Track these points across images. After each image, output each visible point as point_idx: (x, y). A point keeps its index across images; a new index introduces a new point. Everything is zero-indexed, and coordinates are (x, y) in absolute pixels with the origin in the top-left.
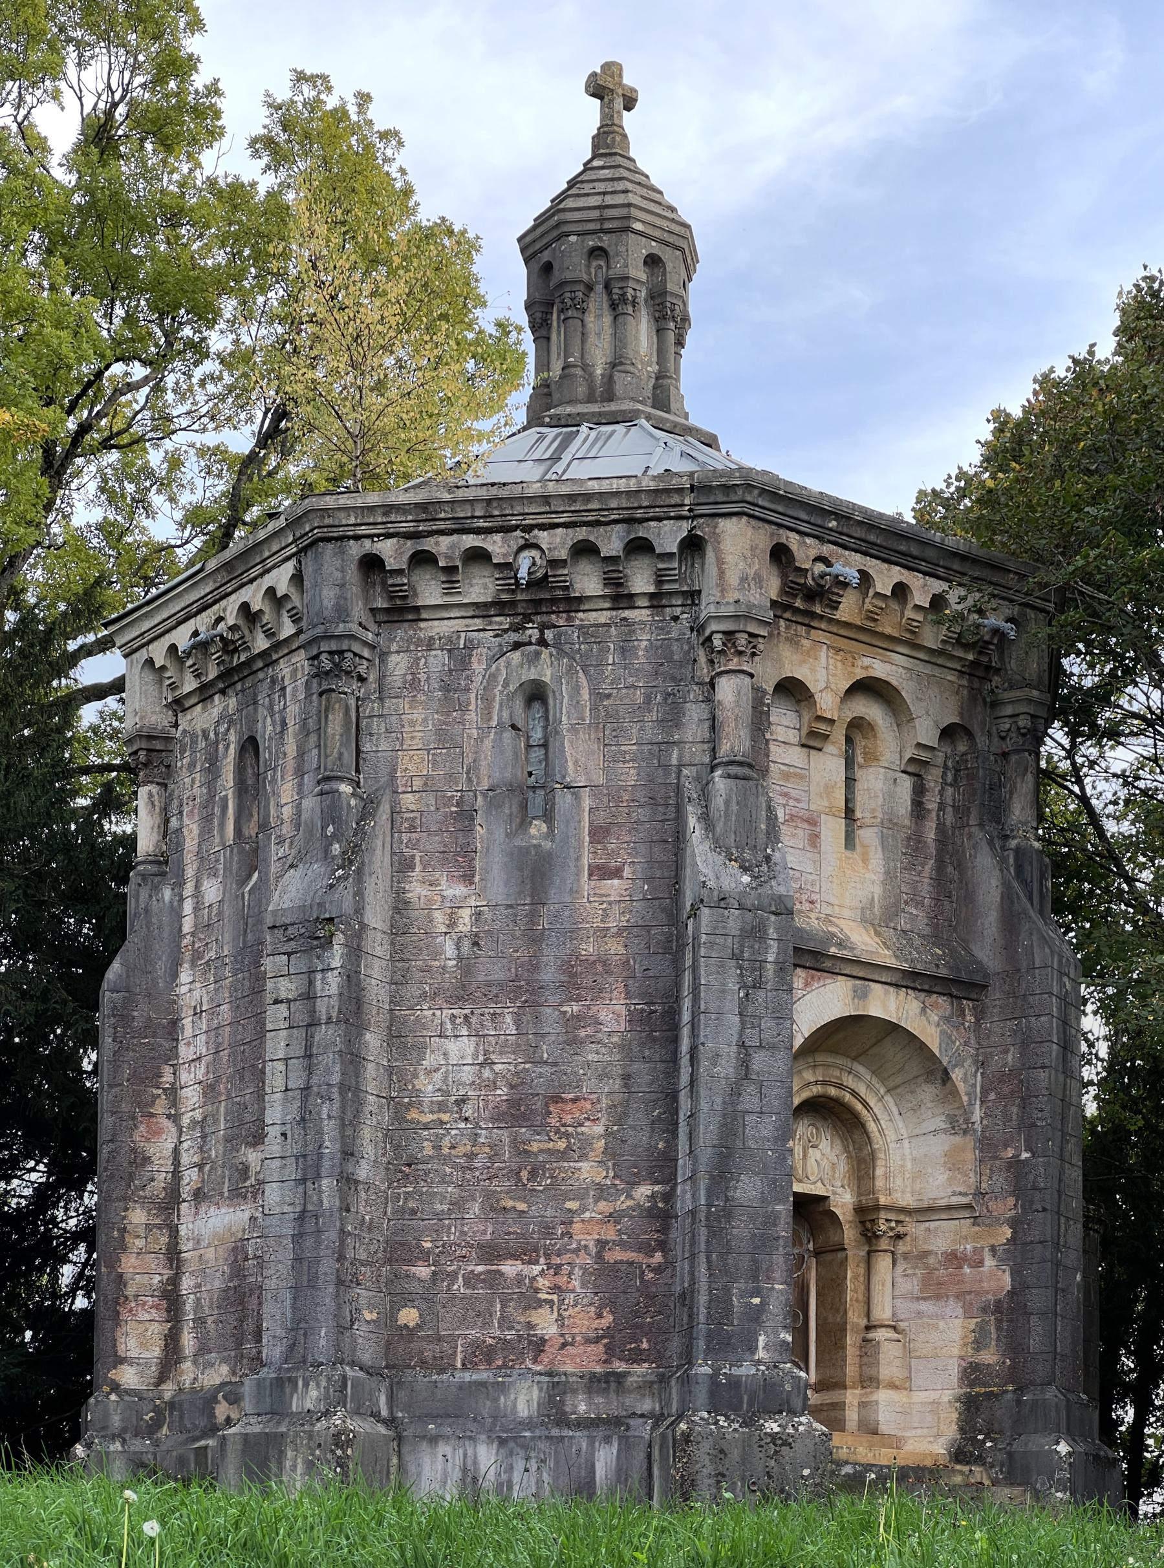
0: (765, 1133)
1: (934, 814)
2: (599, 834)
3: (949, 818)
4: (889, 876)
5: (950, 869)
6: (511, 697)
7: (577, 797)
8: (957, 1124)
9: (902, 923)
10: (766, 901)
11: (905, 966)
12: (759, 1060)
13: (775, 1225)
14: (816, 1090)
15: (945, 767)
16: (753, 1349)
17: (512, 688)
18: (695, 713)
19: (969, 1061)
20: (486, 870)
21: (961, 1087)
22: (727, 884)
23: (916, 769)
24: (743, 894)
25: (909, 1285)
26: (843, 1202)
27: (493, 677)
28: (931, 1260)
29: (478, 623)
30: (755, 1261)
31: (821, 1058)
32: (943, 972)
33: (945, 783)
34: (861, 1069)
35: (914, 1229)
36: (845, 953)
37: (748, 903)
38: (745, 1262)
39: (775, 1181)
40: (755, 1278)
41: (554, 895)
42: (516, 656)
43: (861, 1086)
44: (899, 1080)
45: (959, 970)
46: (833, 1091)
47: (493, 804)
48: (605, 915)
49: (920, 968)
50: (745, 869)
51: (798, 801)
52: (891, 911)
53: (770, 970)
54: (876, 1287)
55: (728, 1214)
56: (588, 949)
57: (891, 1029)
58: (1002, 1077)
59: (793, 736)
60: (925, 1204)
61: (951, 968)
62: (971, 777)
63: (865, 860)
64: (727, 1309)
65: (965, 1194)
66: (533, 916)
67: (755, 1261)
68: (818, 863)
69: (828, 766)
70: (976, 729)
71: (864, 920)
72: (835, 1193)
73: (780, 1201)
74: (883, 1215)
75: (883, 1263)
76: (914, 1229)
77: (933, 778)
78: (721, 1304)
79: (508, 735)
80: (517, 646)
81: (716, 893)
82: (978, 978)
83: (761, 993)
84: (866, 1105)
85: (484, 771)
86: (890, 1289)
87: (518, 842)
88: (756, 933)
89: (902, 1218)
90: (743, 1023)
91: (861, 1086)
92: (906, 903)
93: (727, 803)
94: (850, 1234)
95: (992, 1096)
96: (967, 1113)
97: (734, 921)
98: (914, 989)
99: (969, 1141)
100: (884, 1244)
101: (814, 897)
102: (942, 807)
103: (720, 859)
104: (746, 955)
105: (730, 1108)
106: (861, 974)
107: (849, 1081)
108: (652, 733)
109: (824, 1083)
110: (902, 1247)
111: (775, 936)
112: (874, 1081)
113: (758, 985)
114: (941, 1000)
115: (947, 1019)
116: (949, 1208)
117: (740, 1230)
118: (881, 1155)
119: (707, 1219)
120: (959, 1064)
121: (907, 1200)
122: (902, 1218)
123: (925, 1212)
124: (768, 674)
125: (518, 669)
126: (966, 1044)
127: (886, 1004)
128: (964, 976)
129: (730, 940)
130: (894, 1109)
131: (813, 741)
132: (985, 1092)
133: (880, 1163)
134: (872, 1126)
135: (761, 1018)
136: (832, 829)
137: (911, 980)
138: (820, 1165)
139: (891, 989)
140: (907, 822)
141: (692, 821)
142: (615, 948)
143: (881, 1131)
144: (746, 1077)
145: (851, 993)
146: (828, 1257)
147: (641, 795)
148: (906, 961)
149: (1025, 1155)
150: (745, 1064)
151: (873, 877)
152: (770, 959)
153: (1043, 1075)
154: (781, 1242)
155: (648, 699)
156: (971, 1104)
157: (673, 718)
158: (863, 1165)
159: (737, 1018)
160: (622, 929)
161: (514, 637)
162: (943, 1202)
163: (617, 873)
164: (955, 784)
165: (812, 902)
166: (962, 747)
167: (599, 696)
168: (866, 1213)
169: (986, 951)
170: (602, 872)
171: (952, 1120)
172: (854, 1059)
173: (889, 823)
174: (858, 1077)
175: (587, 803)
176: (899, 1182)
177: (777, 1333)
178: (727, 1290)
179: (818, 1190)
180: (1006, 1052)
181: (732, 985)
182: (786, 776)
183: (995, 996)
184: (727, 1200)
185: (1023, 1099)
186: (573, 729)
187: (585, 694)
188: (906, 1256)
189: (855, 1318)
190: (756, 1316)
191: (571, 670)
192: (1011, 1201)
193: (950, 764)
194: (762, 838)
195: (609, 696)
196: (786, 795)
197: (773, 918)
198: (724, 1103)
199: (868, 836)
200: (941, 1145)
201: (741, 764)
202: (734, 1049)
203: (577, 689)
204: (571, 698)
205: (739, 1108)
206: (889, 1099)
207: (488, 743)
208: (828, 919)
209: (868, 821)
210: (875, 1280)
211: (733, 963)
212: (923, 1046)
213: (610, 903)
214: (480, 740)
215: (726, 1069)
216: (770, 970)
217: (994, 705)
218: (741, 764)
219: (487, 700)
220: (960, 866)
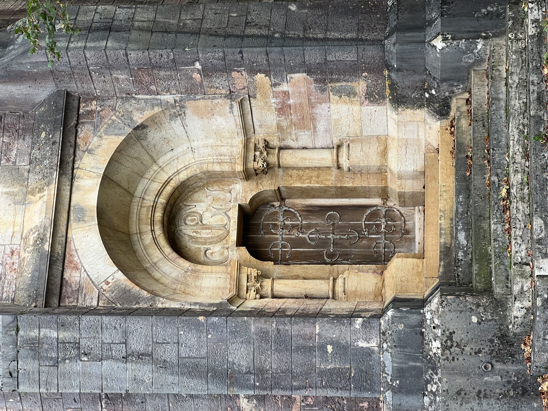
0: (194, 340)
8: (177, 111)
9: (24, 164)
10: (8, 339)
11: (55, 175)
12: (137, 344)
13: (267, 332)
14: (158, 231)
16: (369, 352)
19: (127, 105)
21: (148, 113)
25: (305, 138)
26: (243, 192)
28: (284, 124)
30: (298, 349)
31: (134, 228)
32: (58, 137)
34: (140, 188)
35: (260, 135)
36: (49, 235)
37: (12, 353)
38: (298, 358)
39: (232, 332)
40: (311, 349)
43: (151, 192)
44: (146, 157)
45: (56, 121)
46: (159, 215)
49: (56, 160)
53: (64, 335)
54: (307, 164)
55: (260, 372)
57: (107, 180)
58: (138, 82)
60: (241, 131)
61: (55, 129)
64: (339, 373)
65: (231, 107)
67: (298, 349)
71: (23, 202)
72: (236, 200)
73: (247, 328)
74: (251, 165)
75: (288, 158)
76: (260, 135)
78: (334, 378)
81: (5, 380)
82: (62, 103)
83: (83, 342)
84: (167, 183)
86: (308, 157)
88: (35, 346)
89: (252, 146)
90: (108, 358)
91: (151, 192)
92: (8, 160)
94: (267, 185)
95: (153, 88)
96: (167, 106)
97: (27, 365)
98: (74, 161)
99: (190, 105)
100: (273, 159)
101: (8, 251)
104: (54, 355)
105: (176, 369)
106: (65, 216)
107: (150, 199)
109: (152, 223)
110: (275, 142)
111: (36, 331)
112: (148, 176)
113: (77, 345)
114: (81, 135)
115: (96, 128)
116: (243, 115)
117: (273, 362)
118: (205, 168)
119: (265, 389)
120: (129, 115)
121: (239, 141)
122: (252, 146)
123: (246, 130)
126: (114, 109)
127: (87, 191)
128: (60, 117)
129: (43, 369)
130: (169, 155)
132: (150, 92)
133: (210, 168)
134: (183, 176)
135: (103, 343)
137: (66, 167)
138: (214, 216)
139: (76, 184)
143: (186, 168)
144: (150, 355)
145: (81, 224)
146: (284, 194)
148: (51, 174)
149: (198, 65)
150: (140, 356)
152: (55, 335)
153: (133, 55)
154: (281, 327)
156: (160, 104)
158: (212, 179)
159: (105, 363)
162: (239, 120)
165: (12, 253)
168: (248, 175)
169: (42, 92)
171: (174, 117)
172: (132, 195)
174: (145, 192)
176: (224, 150)
177: (355, 331)
178: (322, 373)
179: (234, 214)
180: (117, 79)
181: (78, 366)
183: (74, 87)
184: (249, 372)
185: (153, 68)
188: (281, 140)
189: (330, 180)
190: (342, 349)
192: (234, 74)
197: (21, 333)
198: (172, 374)
200: (193, 121)
202: (129, 365)
205: (175, 362)
206: (161, 161)
208: (25, 239)
210: (301, 164)
211: (61, 365)
212: (119, 151)
215: (145, 371)
216: (64, 335)
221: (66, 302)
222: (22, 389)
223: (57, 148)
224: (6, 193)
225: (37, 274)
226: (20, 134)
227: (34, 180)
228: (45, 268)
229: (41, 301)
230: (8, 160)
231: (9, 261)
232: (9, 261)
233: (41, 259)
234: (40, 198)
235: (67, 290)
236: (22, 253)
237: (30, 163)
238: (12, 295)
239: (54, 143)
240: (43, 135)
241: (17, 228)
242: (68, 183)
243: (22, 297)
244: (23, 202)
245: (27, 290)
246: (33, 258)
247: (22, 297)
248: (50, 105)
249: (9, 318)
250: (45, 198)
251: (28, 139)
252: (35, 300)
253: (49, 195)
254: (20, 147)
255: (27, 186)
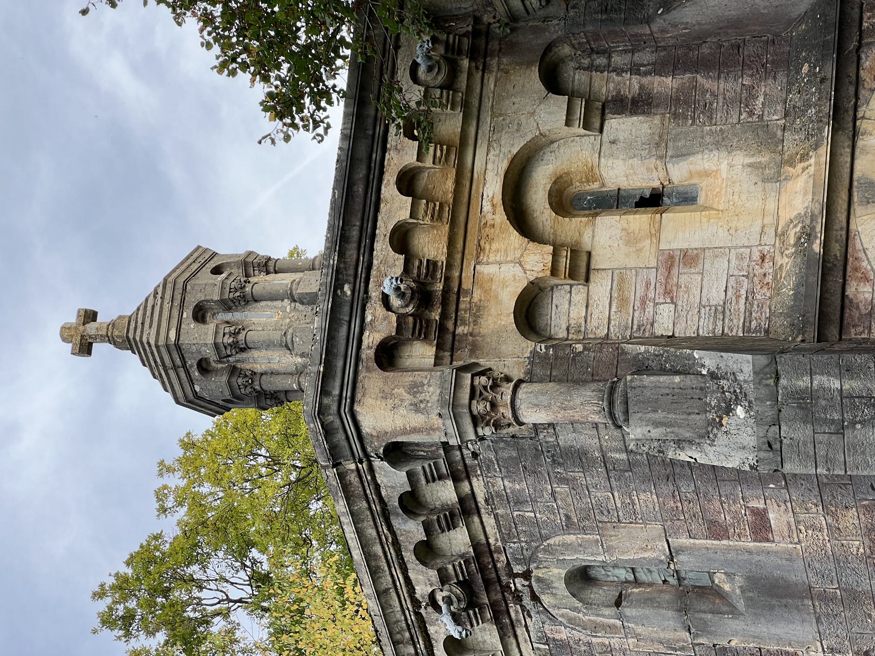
1: (646, 80)
2: (717, 531)
3: (646, 57)
4: (721, 143)
5: (705, 50)
6: (587, 604)
7: (681, 550)
9: (775, 118)
10: (763, 391)
11: (827, 131)
15: (591, 68)
17: (580, 605)
18: (566, 438)
20: (779, 640)
22: (749, 437)
23: (594, 113)
24: (759, 421)
27: (570, 620)
29: (521, 631)
32: (830, 70)
33: (608, 68)
36: (819, 228)
37: (770, 413)
41: (798, 575)
42: (546, 599)
47: (704, 629)
48: (813, 527)
49: (827, 108)
50: (729, 411)
51: (648, 284)
52: (765, 137)
56: (857, 545)
59: (579, 294)
61: (824, 58)
62: (597, 37)
63: (707, 174)
66: (826, 598)
68: (718, 251)
69: (607, 236)
70: (541, 41)
71: (778, 178)
77: (605, 85)
79: (628, 611)
80: (535, 598)
81: (762, 455)
85: (669, 635)
87: (741, 605)
88: (807, 404)
92: (751, 113)
93: (657, 424)
97: (795, 432)
98: (856, 108)
101: (756, 256)
102: (635, 69)
103: (721, 439)
104: (836, 416)
106: (844, 195)
108: (597, 476)
111: (807, 379)
124: (511, 353)
125: (558, 598)
128: (832, 36)
129: (819, 437)
131: (577, 266)
136: (679, 229)
139: (860, 143)
140: (657, 120)
141: (683, 456)
142: (851, 519)
147: (667, 489)
148: (821, 130)
151: (724, 166)
152: (837, 385)
155: (563, 480)
157: (578, 457)
160: (827, 512)
161: (527, 601)
163: (761, 516)
164: (607, 53)
165: (763, 258)
166: (566, 50)
167: (569, 526)
170: (761, 527)
173: (662, 147)
175: (683, 541)
182: (623, 302)
186: (608, 550)
187: (570, 538)
191: (548, 550)
193: (586, 62)
194: (690, 381)
195: (568, 517)
196: (643, 303)
197: (783, 382)
199: (679, 173)
201: (611, 404)
203: (567, 546)
204: (576, 552)
207: (640, 629)
208: (781, 235)
209: (662, 174)
211: (848, 433)
213: (798, 522)
214: (637, 636)
217: (513, 18)
218: (611, 404)
219: (596, 628)
220: (701, 37)
221: (853, 333)
222: (788, 468)
223: (829, 88)
224: (750, 165)
225: (802, 290)
226: (767, 71)
227: (792, 142)
228: (815, 279)
229: (812, 332)
230: (751, 113)
231: (759, 271)
232: (759, 271)
233: (808, 267)
234: (804, 169)
235: (852, 314)
236: (778, 258)
237: (786, 116)
238: (765, 325)
239: (823, 80)
240: (805, 68)
241: (768, 220)
242: (848, 143)
243: (781, 326)
244: (774, 177)
245: (788, 315)
246: (795, 265)
247: (781, 326)
248: (814, 18)
249: (763, 360)
250: (812, 170)
251: (782, 78)
252: (802, 331)
253: (817, 164)
254: (769, 90)
255: (782, 153)
